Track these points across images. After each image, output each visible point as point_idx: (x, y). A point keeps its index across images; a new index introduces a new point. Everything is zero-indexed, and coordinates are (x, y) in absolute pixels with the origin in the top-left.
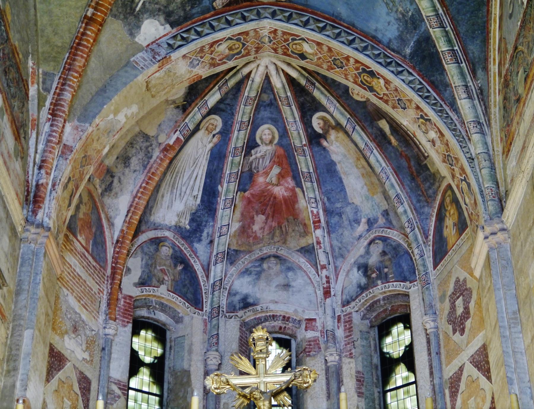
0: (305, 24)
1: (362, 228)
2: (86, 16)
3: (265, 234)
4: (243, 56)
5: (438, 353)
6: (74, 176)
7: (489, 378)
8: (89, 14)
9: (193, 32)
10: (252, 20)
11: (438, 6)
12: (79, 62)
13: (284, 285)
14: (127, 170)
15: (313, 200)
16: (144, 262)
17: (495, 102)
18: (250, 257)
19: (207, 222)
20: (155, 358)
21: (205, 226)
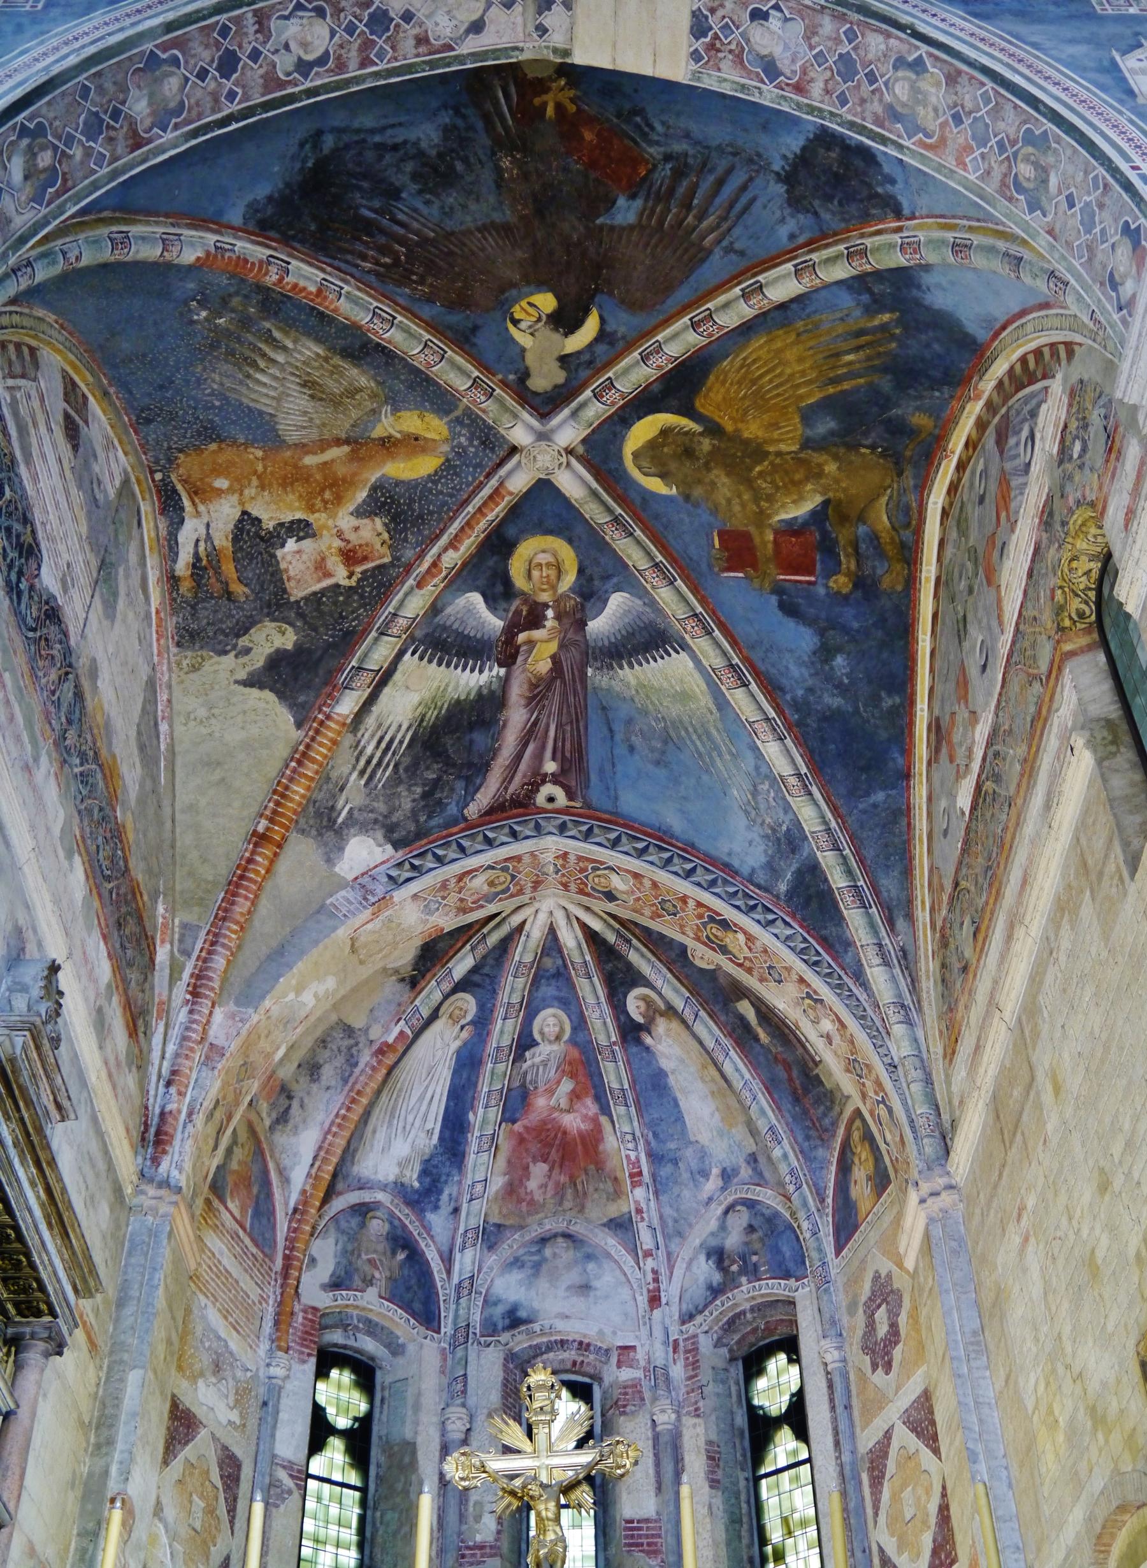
0: (615, 844)
1: (712, 1185)
2: (255, 831)
3: (549, 1195)
4: (512, 896)
5: (848, 1407)
6: (224, 1098)
7: (936, 1451)
8: (261, 829)
9: (430, 856)
10: (527, 837)
11: (829, 815)
12: (242, 906)
13: (581, 1287)
14: (315, 1087)
15: (629, 1137)
16: (339, 1247)
17: (927, 971)
18: (522, 1236)
19: (448, 1175)
20: (356, 1419)
21: (446, 1182)
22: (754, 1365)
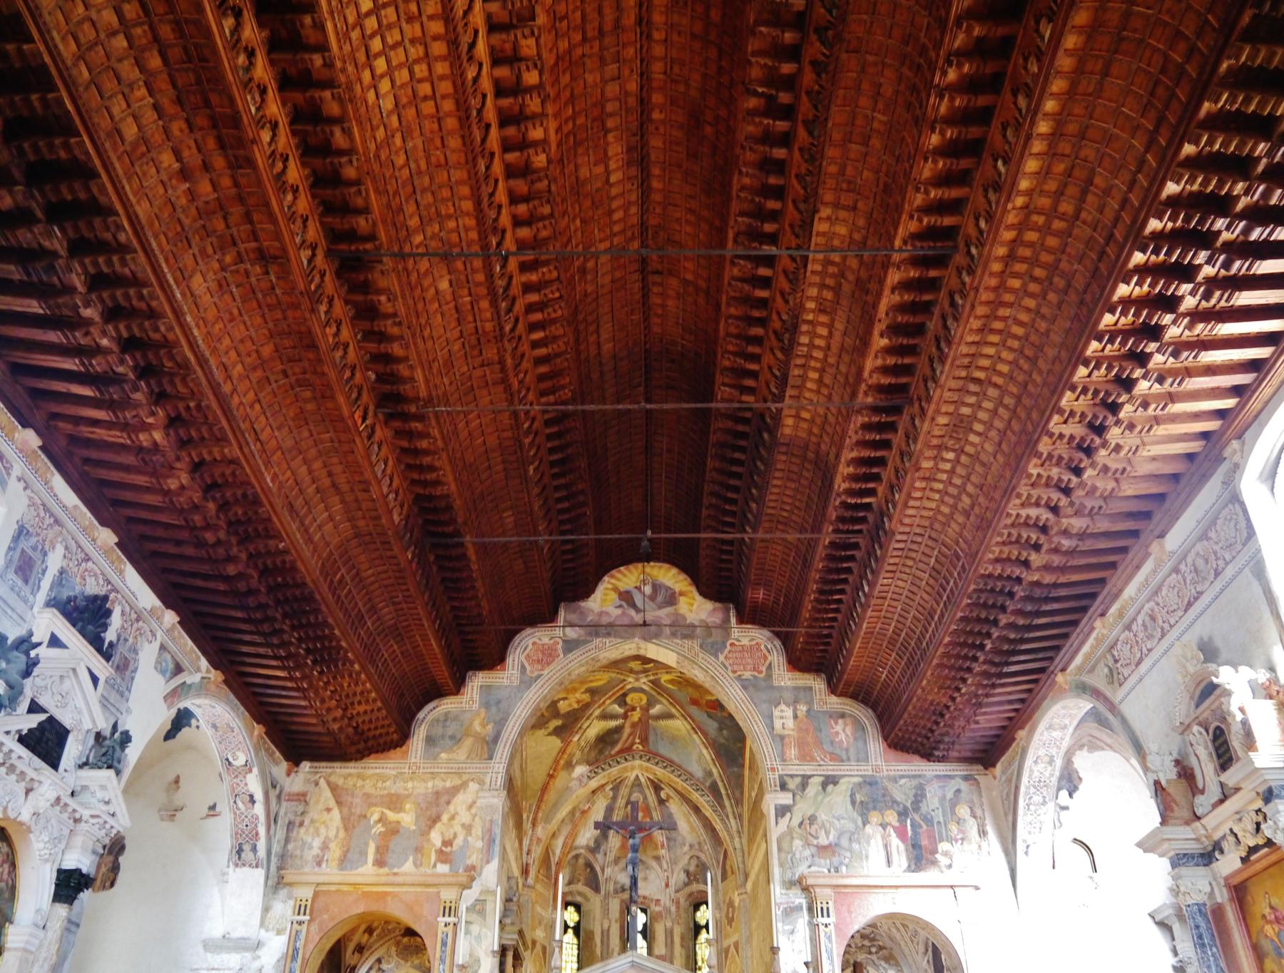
0: (657, 764)
1: (686, 848)
12: (546, 798)
22: (696, 907)
